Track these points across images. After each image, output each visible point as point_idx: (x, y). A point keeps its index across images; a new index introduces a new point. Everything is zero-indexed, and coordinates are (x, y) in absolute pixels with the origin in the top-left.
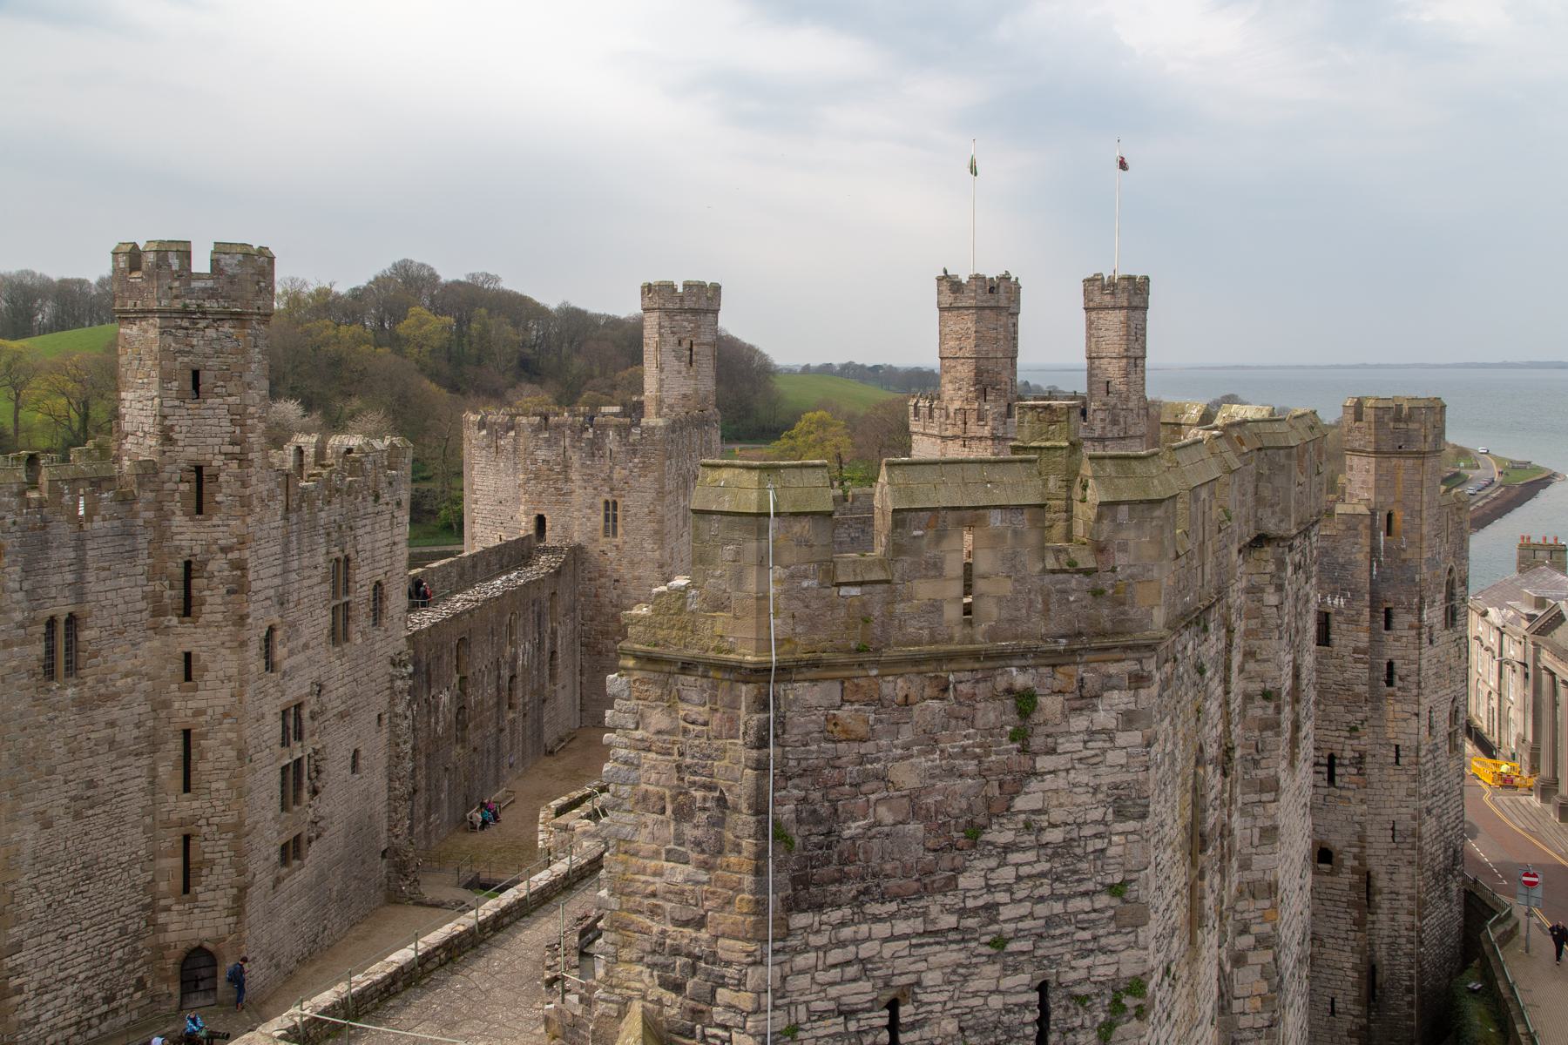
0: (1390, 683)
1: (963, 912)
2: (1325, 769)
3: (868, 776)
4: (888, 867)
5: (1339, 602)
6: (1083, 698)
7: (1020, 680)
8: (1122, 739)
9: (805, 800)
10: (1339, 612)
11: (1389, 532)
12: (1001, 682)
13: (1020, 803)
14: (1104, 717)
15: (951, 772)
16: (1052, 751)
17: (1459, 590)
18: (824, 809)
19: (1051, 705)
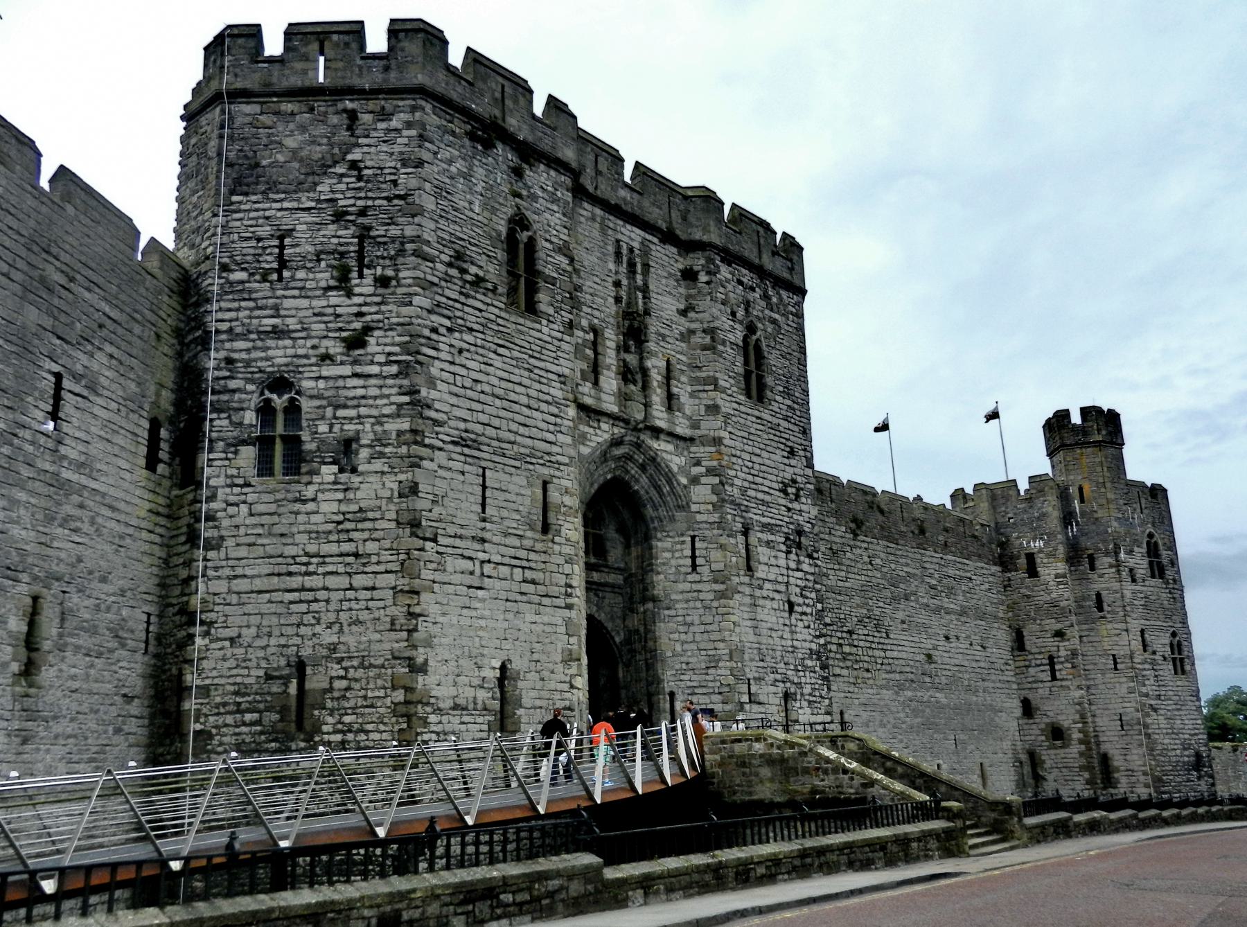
0: (1100, 609)
1: (319, 201)
2: (1048, 667)
3: (272, 142)
4: (280, 179)
5: (1039, 544)
6: (384, 115)
7: (349, 105)
8: (405, 133)
9: (241, 151)
10: (1041, 551)
11: (1082, 501)
12: (340, 106)
13: (349, 157)
14: (394, 123)
15: (313, 142)
16: (367, 136)
17: (1165, 554)
18: (251, 154)
19: (366, 118)
